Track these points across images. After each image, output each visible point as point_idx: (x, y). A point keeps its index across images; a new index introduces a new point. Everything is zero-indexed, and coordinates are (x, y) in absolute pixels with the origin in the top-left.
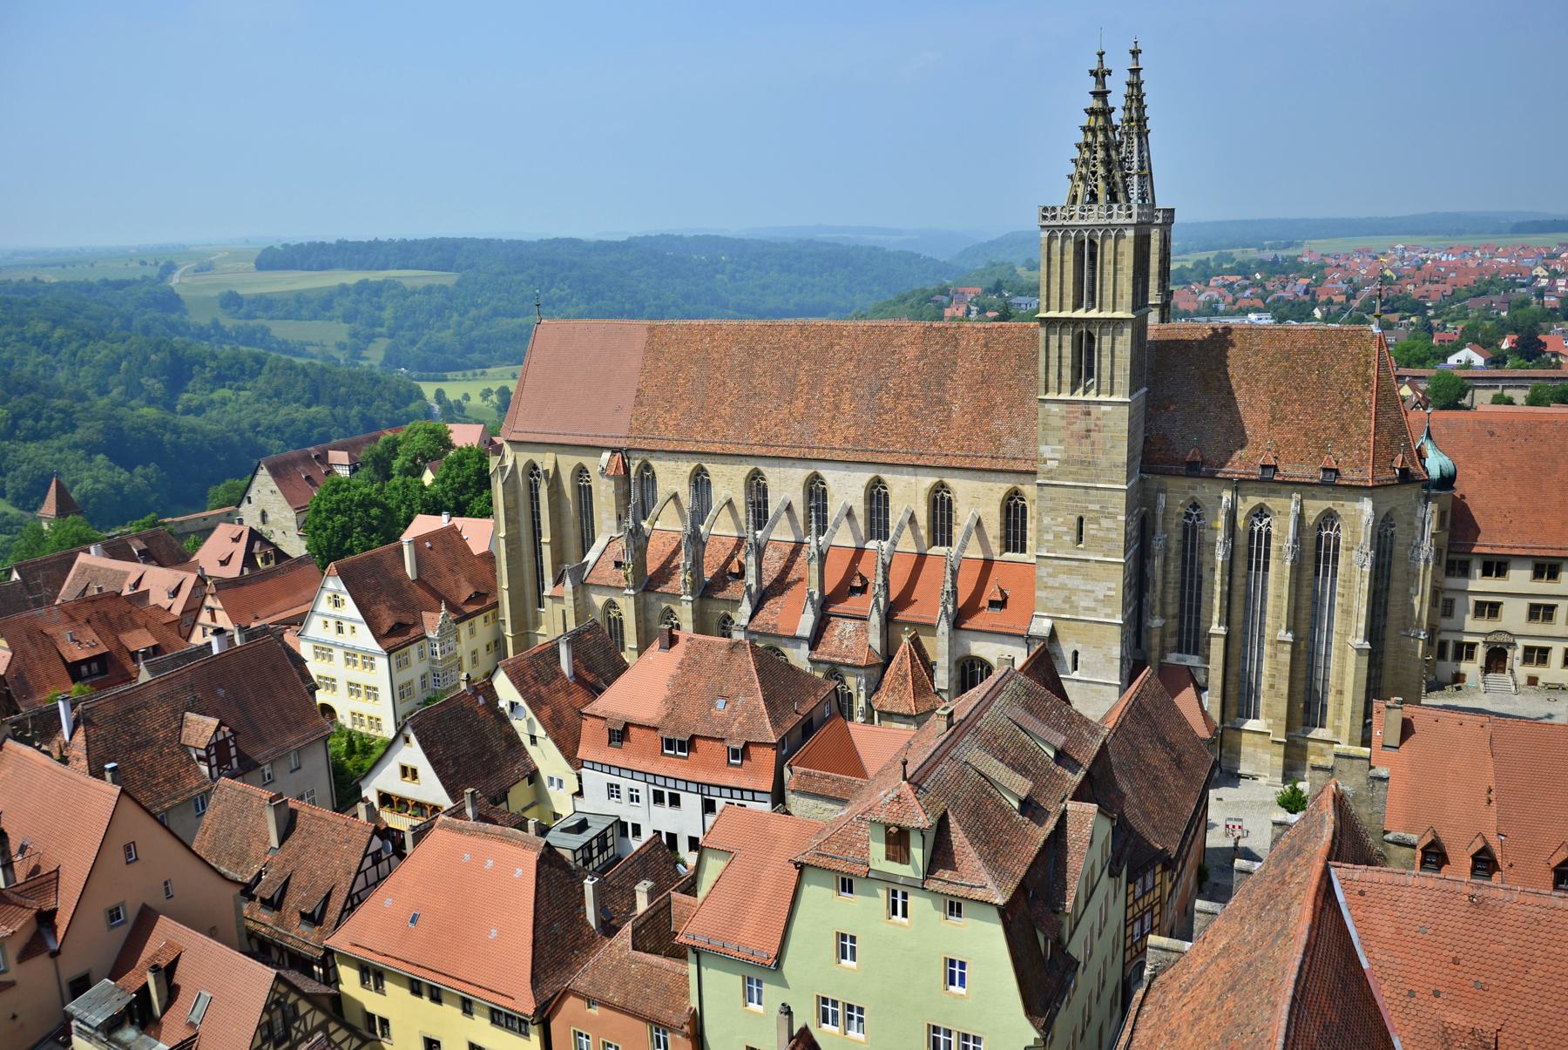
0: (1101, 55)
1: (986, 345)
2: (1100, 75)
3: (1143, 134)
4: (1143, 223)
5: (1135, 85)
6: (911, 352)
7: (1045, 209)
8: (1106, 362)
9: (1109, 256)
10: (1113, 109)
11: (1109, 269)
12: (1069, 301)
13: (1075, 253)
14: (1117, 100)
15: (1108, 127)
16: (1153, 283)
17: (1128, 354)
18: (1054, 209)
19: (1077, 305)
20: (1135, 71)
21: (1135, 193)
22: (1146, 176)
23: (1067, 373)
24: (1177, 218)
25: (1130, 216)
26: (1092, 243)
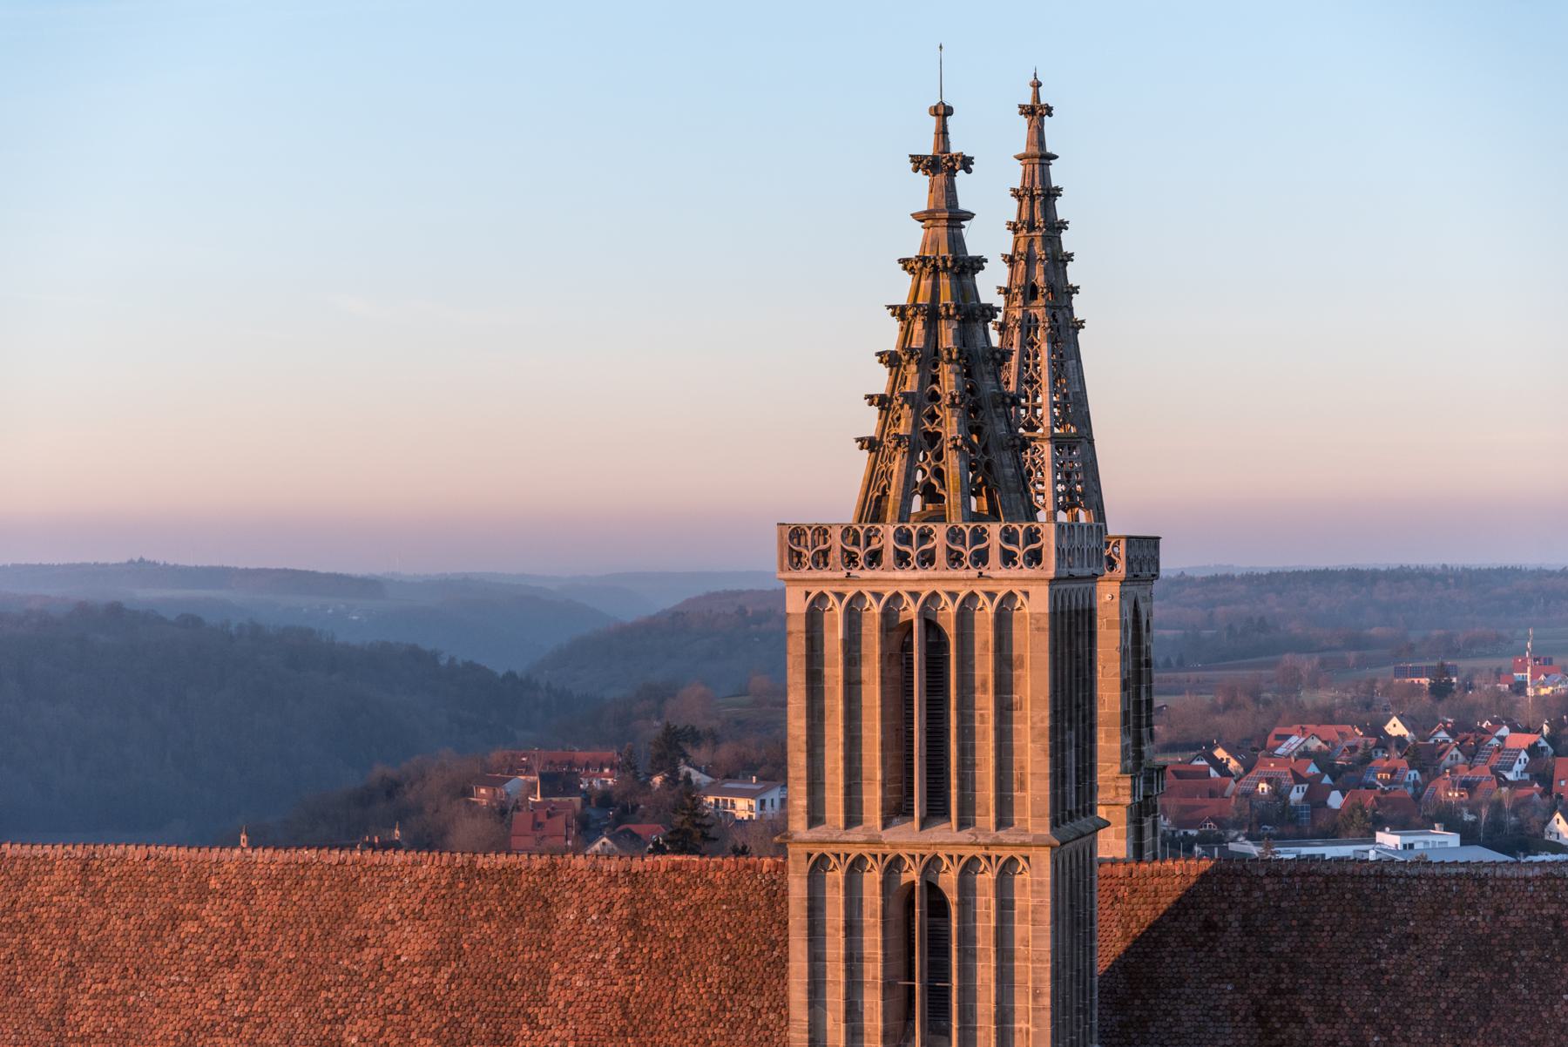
0: (943, 112)
1: (634, 922)
2: (942, 165)
3: (1065, 331)
4: (1071, 578)
5: (1039, 199)
6: (412, 942)
7: (797, 533)
8: (985, 971)
9: (985, 667)
10: (978, 264)
11: (985, 703)
12: (873, 797)
13: (886, 658)
14: (990, 236)
15: (973, 314)
16: (1109, 745)
17: (1046, 945)
18: (822, 531)
19: (897, 810)
20: (1039, 158)
21: (1046, 489)
22: (1076, 438)
23: (873, 1003)
24: (1170, 562)
25: (1035, 558)
26: (931, 626)
